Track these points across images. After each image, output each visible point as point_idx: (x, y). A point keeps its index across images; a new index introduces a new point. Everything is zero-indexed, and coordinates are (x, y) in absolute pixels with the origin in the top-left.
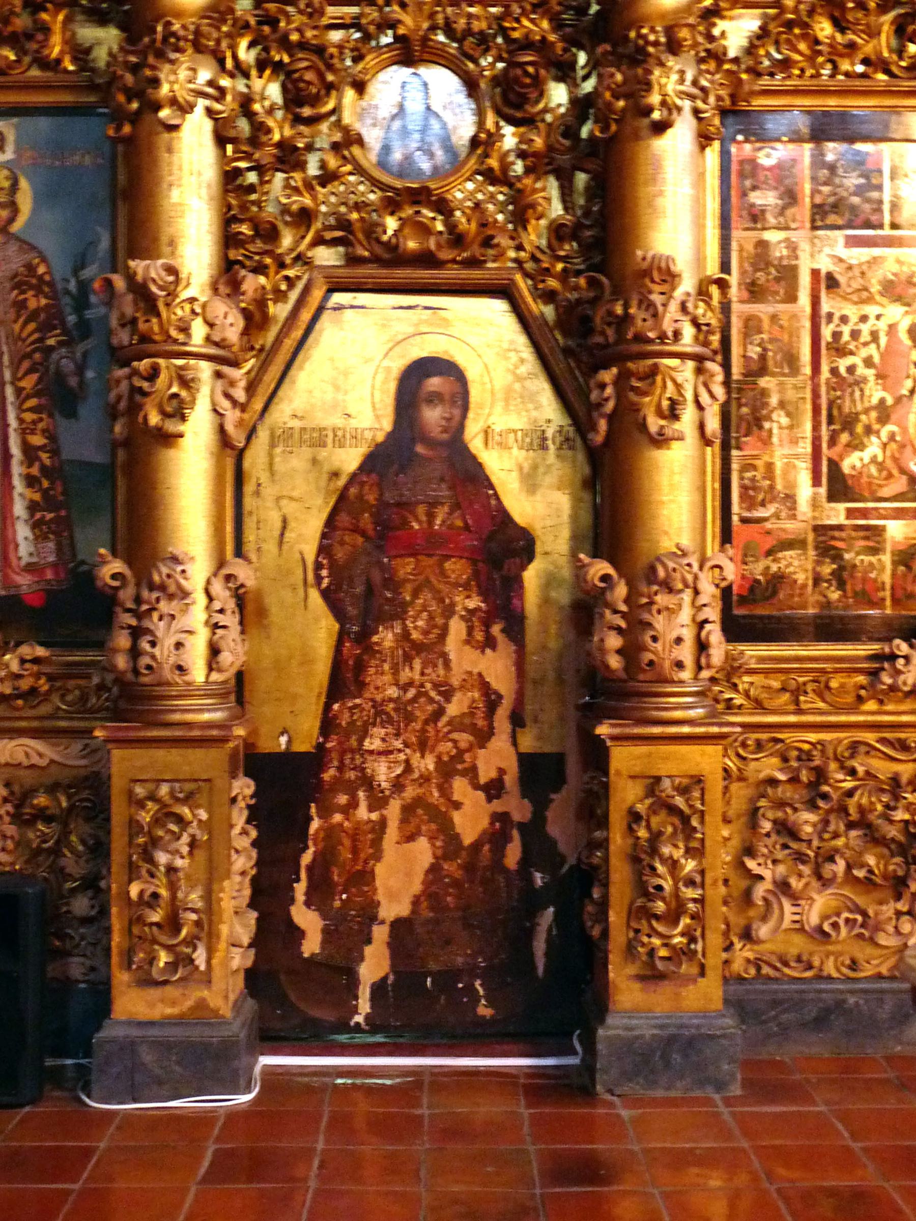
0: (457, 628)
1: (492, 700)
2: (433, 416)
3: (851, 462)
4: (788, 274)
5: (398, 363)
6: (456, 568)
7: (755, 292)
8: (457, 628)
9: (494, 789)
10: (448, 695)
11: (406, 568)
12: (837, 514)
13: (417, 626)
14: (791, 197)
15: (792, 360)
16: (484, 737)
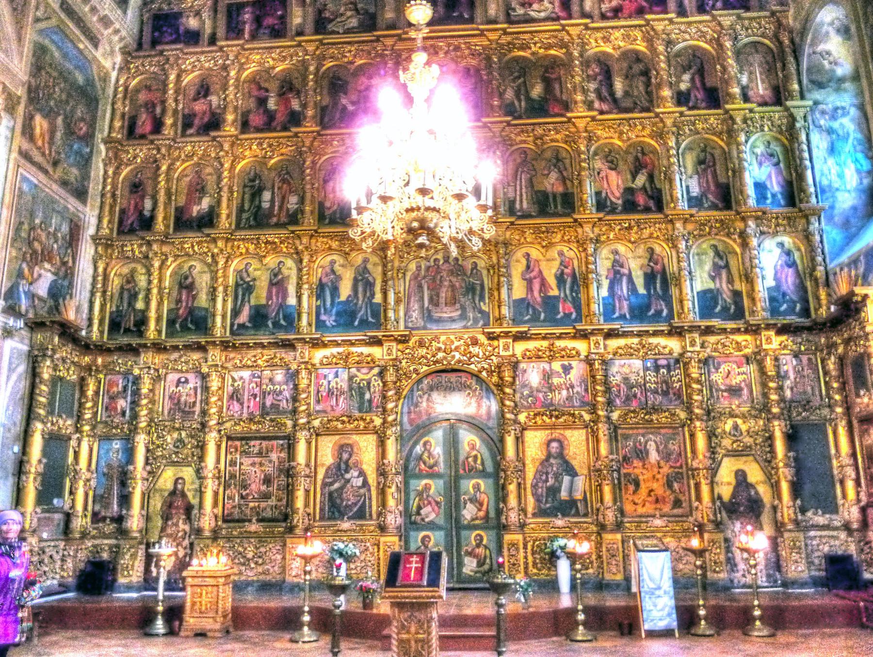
0: (181, 522)
1: (186, 533)
2: (179, 486)
3: (244, 493)
4: (235, 463)
5: (174, 478)
6: (181, 511)
7: (230, 465)
8: (181, 522)
9: (185, 548)
10: (178, 532)
11: (174, 512)
12: (242, 502)
13: (175, 521)
14: (236, 450)
15: (236, 476)
16: (184, 539)
